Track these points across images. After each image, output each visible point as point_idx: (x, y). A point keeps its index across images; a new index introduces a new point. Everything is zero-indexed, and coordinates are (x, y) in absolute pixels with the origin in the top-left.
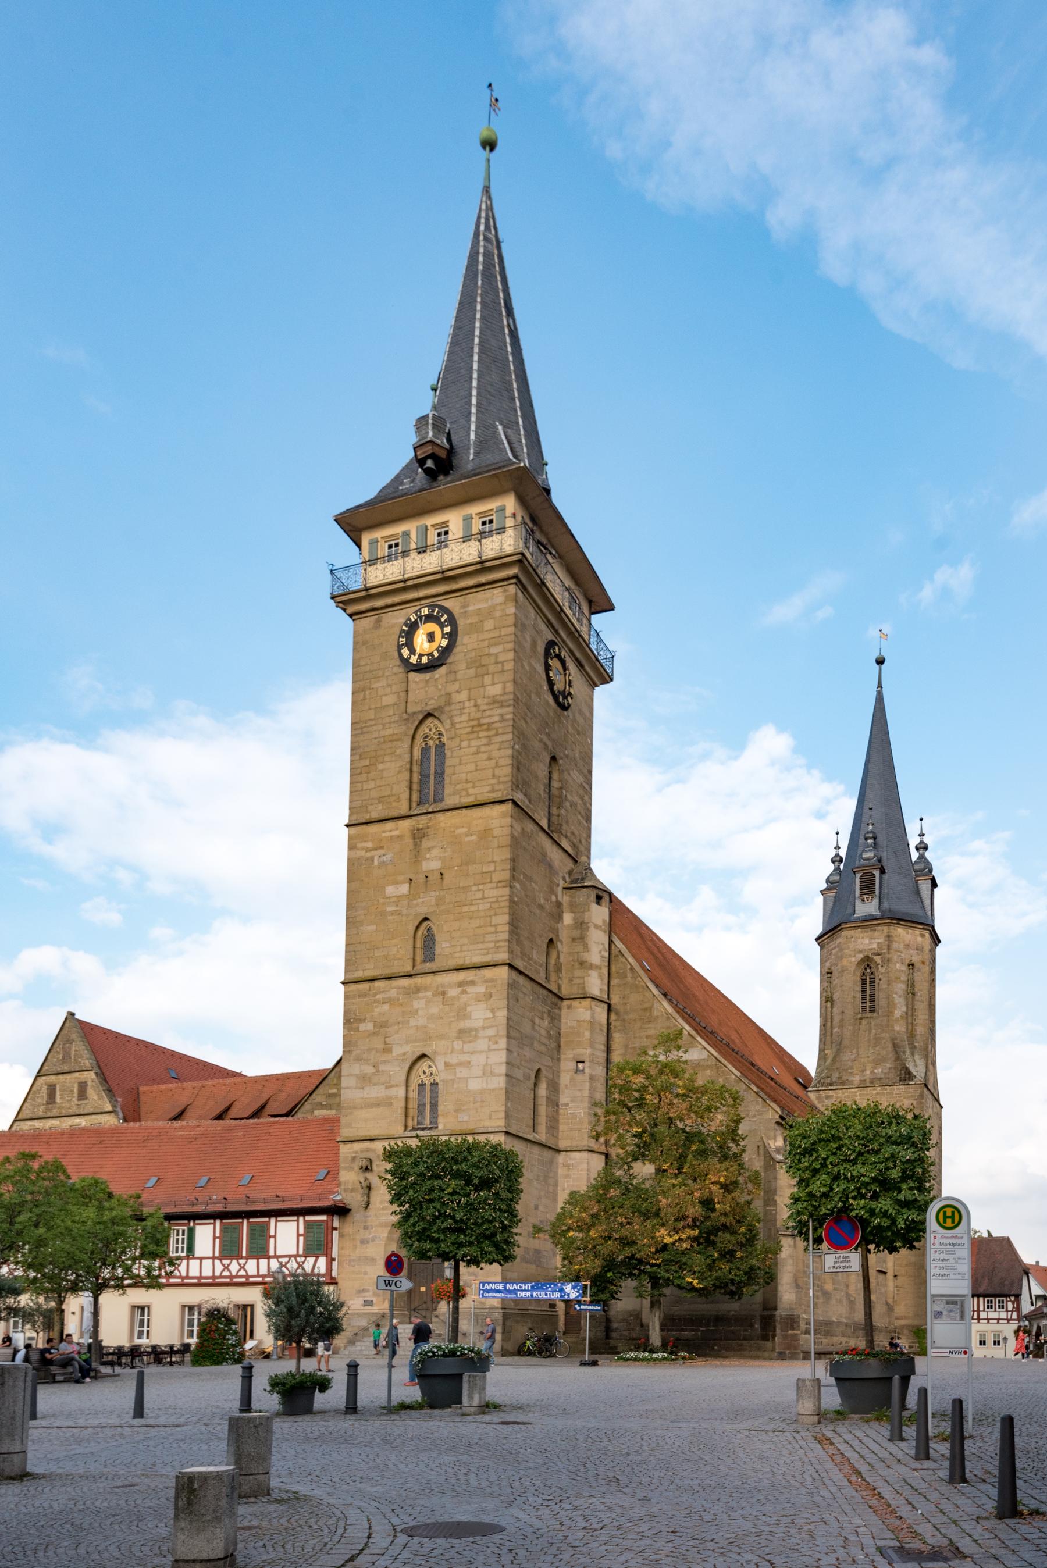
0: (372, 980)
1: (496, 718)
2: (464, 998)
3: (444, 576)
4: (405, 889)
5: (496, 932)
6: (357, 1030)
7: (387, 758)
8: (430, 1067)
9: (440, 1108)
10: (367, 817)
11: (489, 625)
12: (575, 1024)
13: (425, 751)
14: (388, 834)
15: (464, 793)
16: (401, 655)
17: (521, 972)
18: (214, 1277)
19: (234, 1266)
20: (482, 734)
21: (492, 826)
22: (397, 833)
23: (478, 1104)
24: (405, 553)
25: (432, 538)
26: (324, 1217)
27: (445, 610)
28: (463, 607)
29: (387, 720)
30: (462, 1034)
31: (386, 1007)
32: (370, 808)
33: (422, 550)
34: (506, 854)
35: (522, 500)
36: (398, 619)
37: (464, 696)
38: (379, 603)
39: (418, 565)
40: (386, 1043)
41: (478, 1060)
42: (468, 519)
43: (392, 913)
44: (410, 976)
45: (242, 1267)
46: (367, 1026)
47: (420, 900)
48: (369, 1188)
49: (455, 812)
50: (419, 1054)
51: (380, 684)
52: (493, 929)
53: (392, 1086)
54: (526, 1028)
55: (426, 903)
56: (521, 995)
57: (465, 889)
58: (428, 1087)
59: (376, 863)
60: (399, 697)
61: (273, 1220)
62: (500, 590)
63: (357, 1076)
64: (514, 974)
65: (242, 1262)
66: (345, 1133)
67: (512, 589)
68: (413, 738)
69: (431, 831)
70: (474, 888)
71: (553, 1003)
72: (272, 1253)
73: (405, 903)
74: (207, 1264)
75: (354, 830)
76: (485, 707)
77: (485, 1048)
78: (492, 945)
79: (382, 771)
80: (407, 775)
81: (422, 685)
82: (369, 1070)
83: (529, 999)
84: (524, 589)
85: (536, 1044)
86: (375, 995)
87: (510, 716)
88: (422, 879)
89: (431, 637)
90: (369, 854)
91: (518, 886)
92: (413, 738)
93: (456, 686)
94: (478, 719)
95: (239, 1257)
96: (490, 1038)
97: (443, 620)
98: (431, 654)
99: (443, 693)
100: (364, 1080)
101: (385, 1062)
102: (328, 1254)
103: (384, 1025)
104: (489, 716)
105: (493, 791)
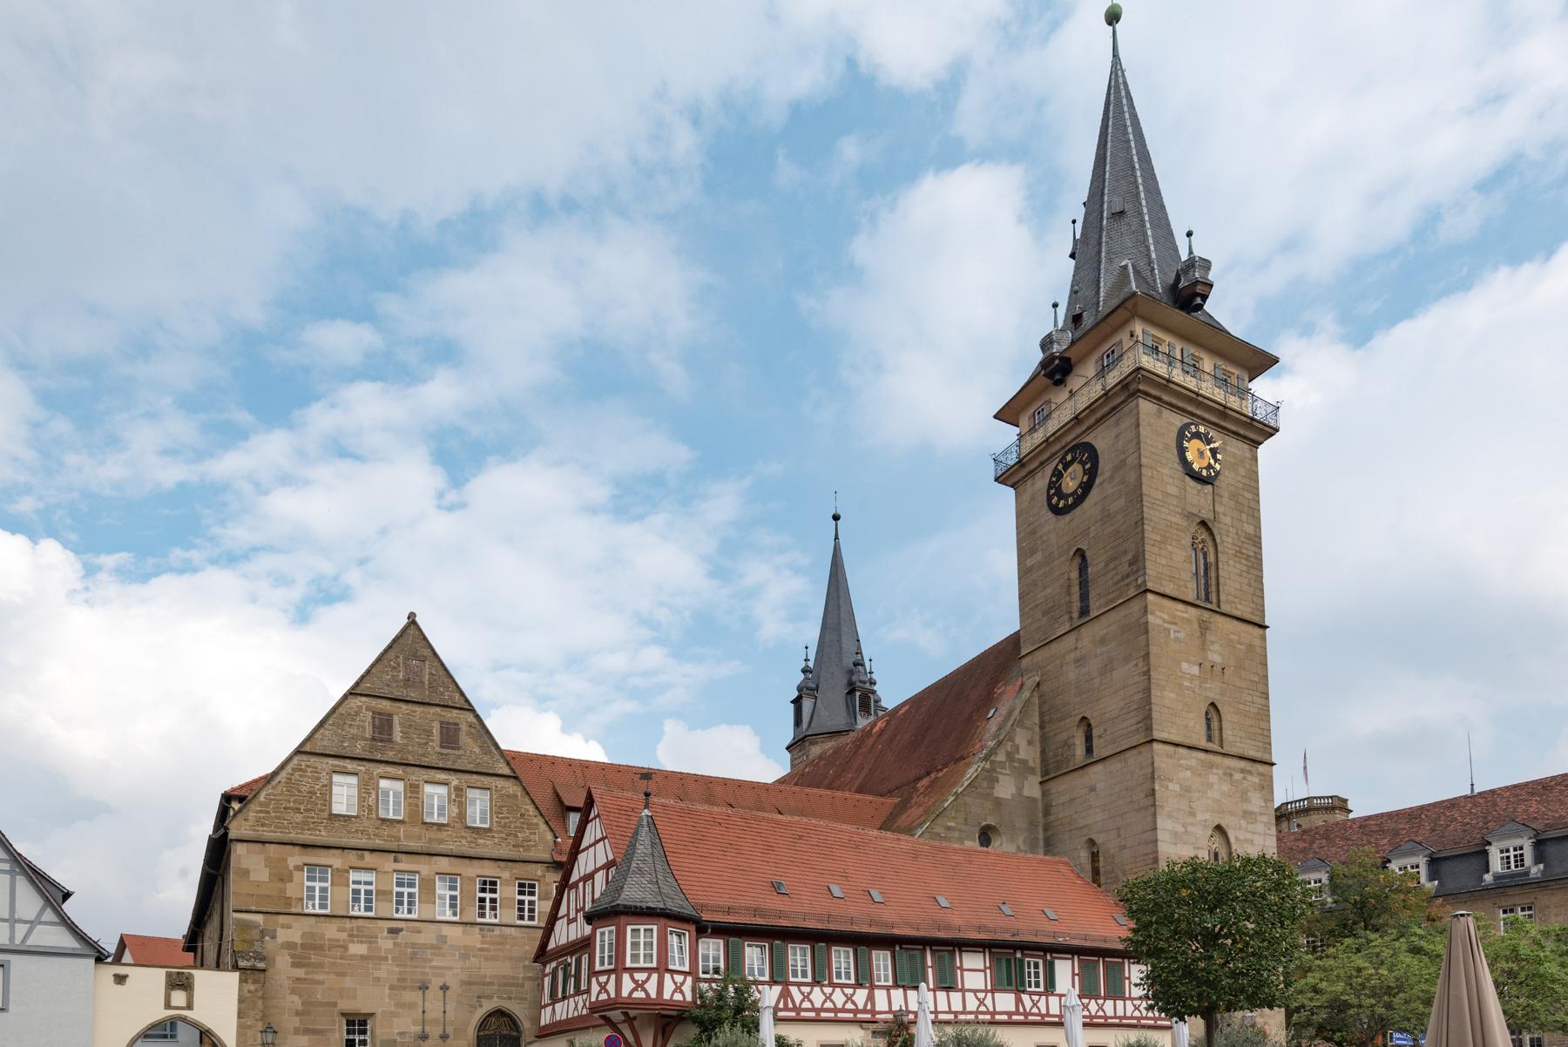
2: (1245, 784)
45: (1101, 1008)
82: (1180, 829)
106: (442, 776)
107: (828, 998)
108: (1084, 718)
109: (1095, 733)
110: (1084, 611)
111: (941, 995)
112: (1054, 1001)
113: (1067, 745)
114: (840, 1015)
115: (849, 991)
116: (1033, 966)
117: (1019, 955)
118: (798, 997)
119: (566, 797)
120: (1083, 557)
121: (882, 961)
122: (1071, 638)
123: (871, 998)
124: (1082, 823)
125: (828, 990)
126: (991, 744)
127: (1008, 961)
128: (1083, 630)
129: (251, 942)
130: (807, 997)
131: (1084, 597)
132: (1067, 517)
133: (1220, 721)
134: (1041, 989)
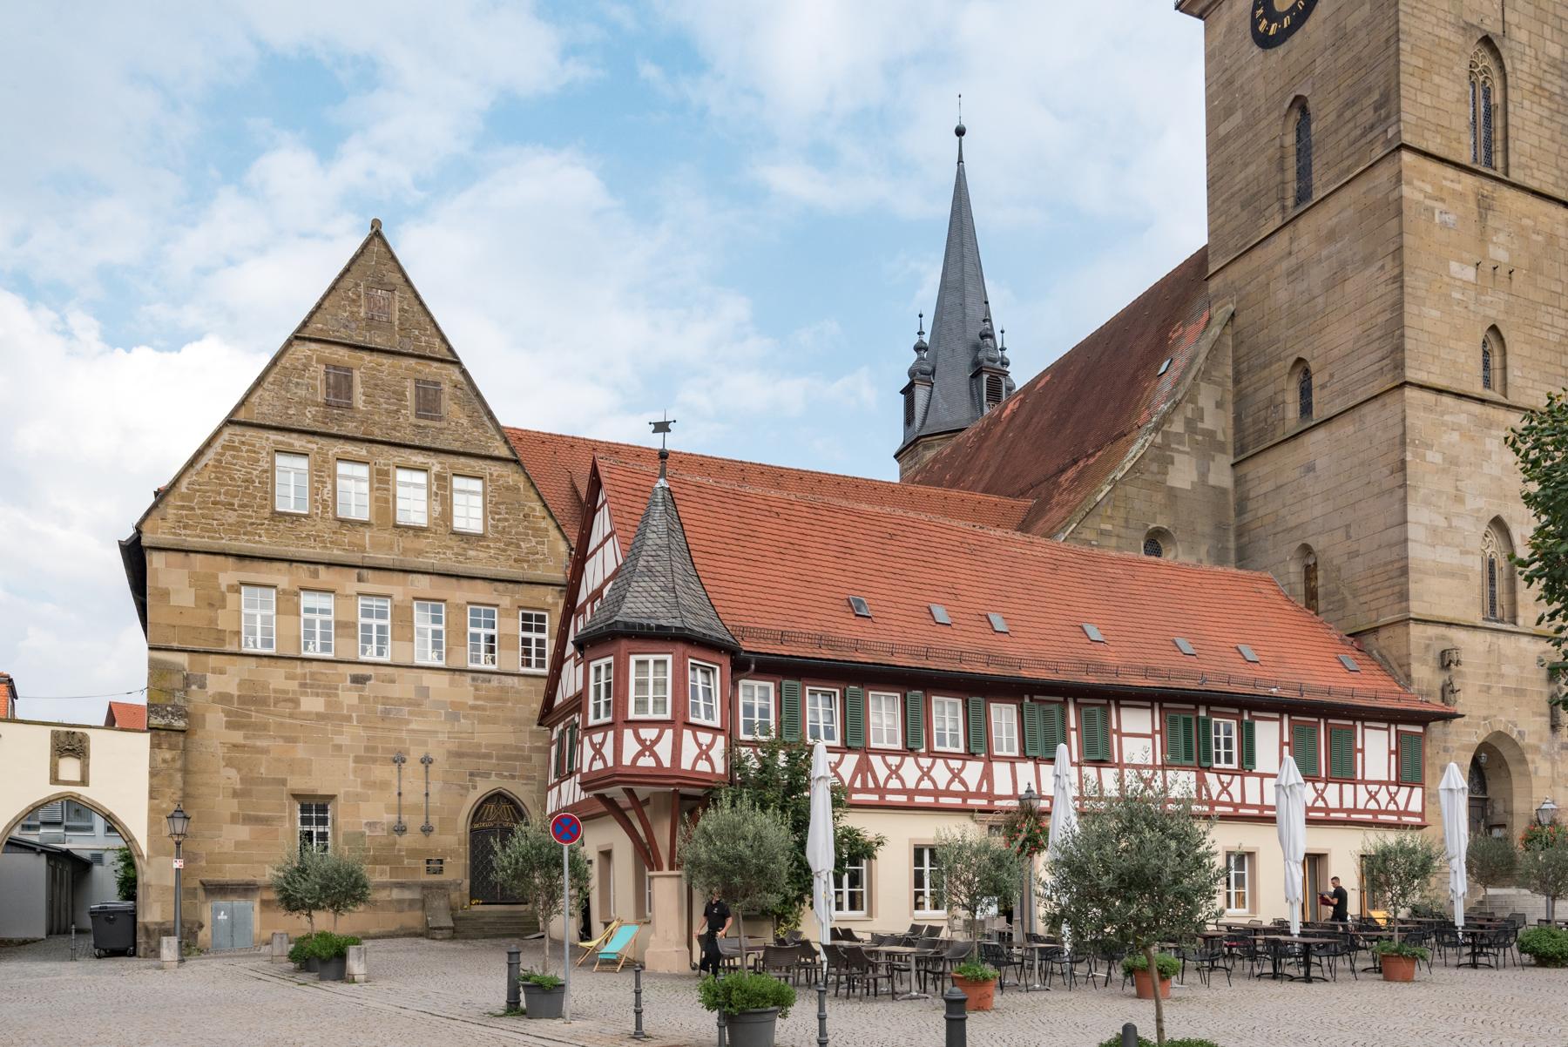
4: (1470, 274)
47: (1489, 298)
55: (1494, 307)
63: (1426, 526)
101: (1458, 515)
102: (1422, 785)
105: (1556, 185)
106: (418, 458)
107: (926, 774)
108: (1300, 360)
109: (1316, 381)
110: (1303, 195)
111: (1090, 771)
112: (1252, 783)
113: (1274, 404)
114: (943, 800)
115: (956, 764)
116: (1225, 727)
117: (1202, 713)
118: (882, 772)
119: (576, 484)
120: (1304, 110)
121: (1003, 718)
122: (1284, 237)
123: (987, 775)
124: (1292, 521)
125: (926, 762)
126: (1164, 407)
127: (1187, 722)
128: (1301, 223)
129: (171, 693)
130: (894, 772)
131: (1304, 173)
132: (1281, 50)
133: (1504, 354)
134: (1235, 765)
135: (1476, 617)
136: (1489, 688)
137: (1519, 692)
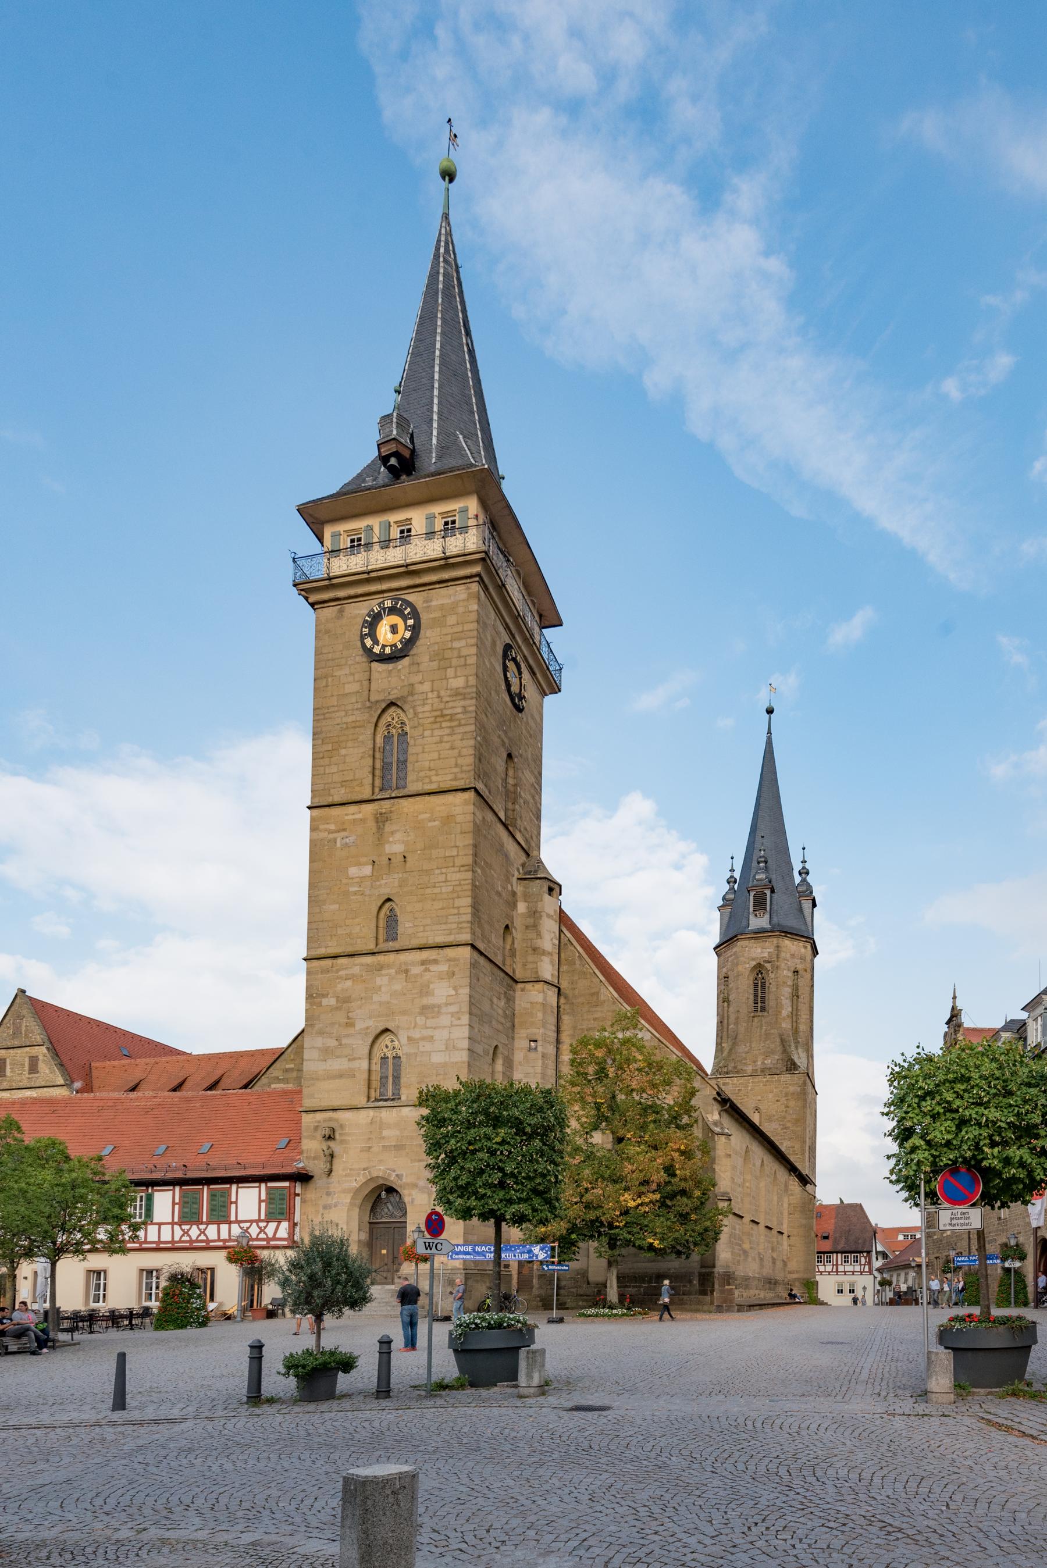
0: (335, 957)
1: (459, 710)
2: (427, 976)
3: (408, 570)
4: (367, 870)
5: (459, 914)
6: (320, 1004)
7: (350, 744)
8: (392, 1041)
9: (403, 1080)
10: (329, 800)
11: (452, 620)
12: (528, 1006)
13: (388, 738)
14: (351, 817)
15: (427, 780)
16: (363, 645)
17: (481, 953)
18: (173, 1242)
19: (194, 1232)
20: (444, 724)
21: (455, 813)
22: (359, 816)
23: (441, 1077)
24: (368, 545)
25: (395, 533)
26: (286, 1184)
27: (409, 604)
28: (426, 601)
29: (350, 707)
30: (425, 1010)
31: (349, 983)
32: (332, 791)
33: (386, 544)
34: (469, 840)
35: (483, 503)
36: (361, 610)
37: (426, 687)
38: (341, 593)
39: (379, 558)
40: (348, 1018)
41: (441, 1035)
42: (431, 518)
43: (355, 893)
44: (373, 954)
45: (203, 1232)
46: (330, 1001)
47: (384, 882)
48: (332, 1156)
49: (418, 798)
50: (382, 1028)
51: (343, 672)
52: (456, 911)
53: (354, 1059)
54: (486, 1007)
55: (389, 885)
56: (482, 975)
57: (428, 872)
58: (391, 1061)
59: (338, 844)
60: (362, 685)
61: (234, 1187)
62: (463, 587)
63: (319, 1049)
64: (476, 955)
65: (202, 1227)
66: (308, 1103)
67: (475, 587)
68: (376, 725)
69: (394, 816)
70: (437, 871)
71: (508, 985)
72: (233, 1218)
73: (369, 883)
74: (166, 1231)
75: (317, 812)
76: (448, 699)
77: (448, 1023)
78: (455, 926)
79: (345, 756)
80: (370, 761)
81: (384, 675)
82: (332, 1043)
83: (488, 979)
84: (486, 588)
85: (494, 1022)
86: (337, 971)
87: (473, 708)
88: (385, 861)
89: (394, 629)
90: (331, 836)
91: (479, 871)
92: (376, 725)
93: (419, 677)
94: (441, 710)
95: (199, 1222)
96: (452, 1015)
97: (406, 612)
98: (395, 645)
99: (406, 683)
100: (327, 1053)
101: (347, 1036)
103: (347, 1000)
104: (452, 708)
105: (455, 779)
135: (362, 1101)
136: (370, 1148)
137: (399, 1147)
